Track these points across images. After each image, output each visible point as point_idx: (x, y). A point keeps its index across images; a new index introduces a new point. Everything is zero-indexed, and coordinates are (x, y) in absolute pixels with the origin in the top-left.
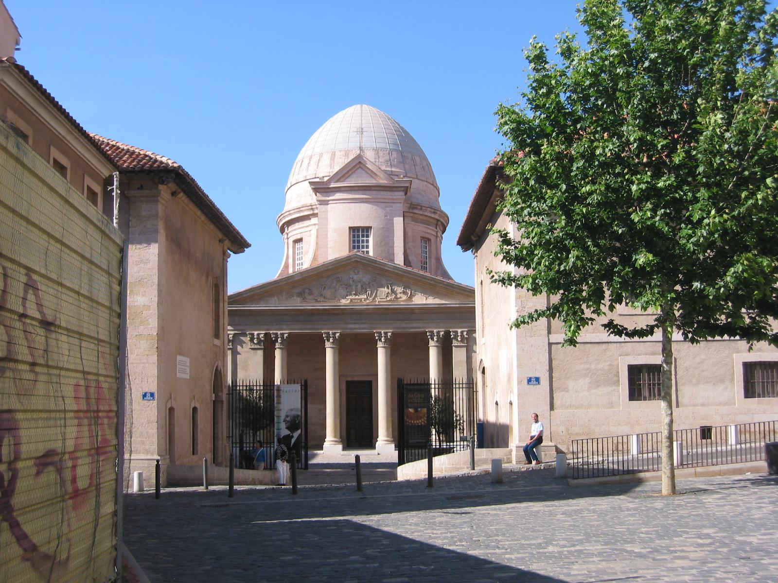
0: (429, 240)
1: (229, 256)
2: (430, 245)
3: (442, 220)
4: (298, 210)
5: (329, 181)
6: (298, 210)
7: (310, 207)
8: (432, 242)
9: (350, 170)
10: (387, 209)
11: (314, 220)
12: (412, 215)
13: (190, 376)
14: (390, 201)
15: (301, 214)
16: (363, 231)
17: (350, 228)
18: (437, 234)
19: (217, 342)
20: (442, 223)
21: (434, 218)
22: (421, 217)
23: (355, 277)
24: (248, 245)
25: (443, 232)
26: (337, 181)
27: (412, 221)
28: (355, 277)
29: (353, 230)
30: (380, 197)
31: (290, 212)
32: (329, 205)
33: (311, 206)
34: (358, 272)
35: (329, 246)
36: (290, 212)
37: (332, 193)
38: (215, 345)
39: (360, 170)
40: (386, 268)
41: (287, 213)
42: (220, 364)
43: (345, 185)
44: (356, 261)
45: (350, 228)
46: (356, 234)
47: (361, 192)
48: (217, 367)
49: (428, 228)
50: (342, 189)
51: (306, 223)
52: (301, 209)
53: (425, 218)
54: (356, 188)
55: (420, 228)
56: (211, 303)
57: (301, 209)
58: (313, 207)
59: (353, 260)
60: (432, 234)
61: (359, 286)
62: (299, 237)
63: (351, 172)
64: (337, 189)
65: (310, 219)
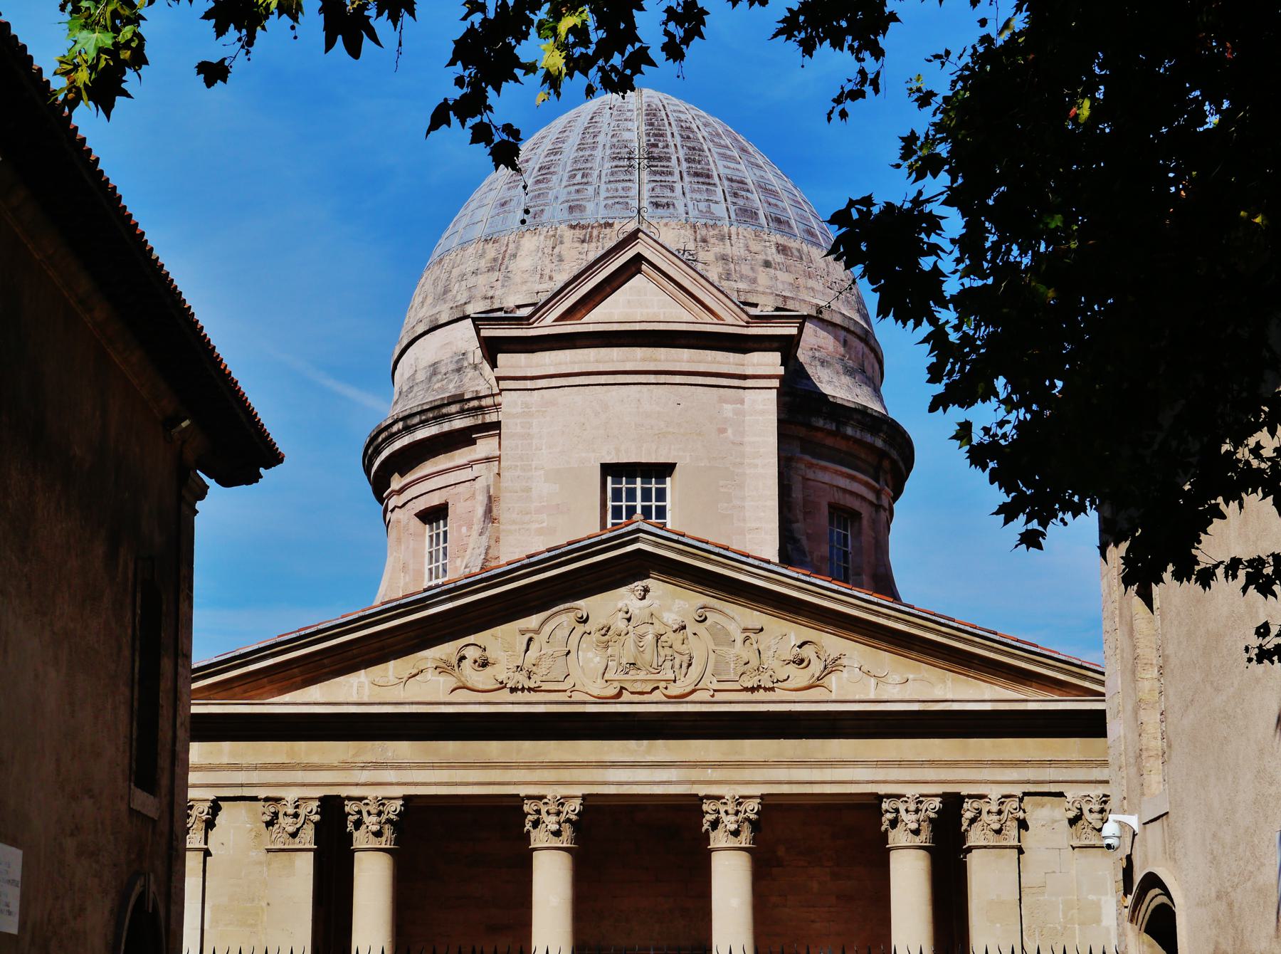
0: (855, 516)
1: (202, 492)
2: (858, 534)
3: (894, 454)
4: (436, 413)
6: (436, 413)
8: (865, 522)
11: (485, 446)
12: (802, 432)
13: (22, 925)
15: (446, 427)
18: (878, 498)
19: (145, 802)
20: (893, 462)
21: (871, 448)
22: (829, 441)
24: (274, 458)
25: (895, 498)
27: (804, 451)
34: (646, 590)
38: (139, 813)
41: (400, 425)
42: (153, 888)
44: (639, 550)
48: (142, 897)
49: (853, 478)
51: (461, 456)
52: (444, 411)
53: (842, 445)
55: (826, 477)
56: (127, 652)
57: (444, 411)
58: (484, 402)
60: (863, 498)
61: (650, 638)
65: (473, 442)
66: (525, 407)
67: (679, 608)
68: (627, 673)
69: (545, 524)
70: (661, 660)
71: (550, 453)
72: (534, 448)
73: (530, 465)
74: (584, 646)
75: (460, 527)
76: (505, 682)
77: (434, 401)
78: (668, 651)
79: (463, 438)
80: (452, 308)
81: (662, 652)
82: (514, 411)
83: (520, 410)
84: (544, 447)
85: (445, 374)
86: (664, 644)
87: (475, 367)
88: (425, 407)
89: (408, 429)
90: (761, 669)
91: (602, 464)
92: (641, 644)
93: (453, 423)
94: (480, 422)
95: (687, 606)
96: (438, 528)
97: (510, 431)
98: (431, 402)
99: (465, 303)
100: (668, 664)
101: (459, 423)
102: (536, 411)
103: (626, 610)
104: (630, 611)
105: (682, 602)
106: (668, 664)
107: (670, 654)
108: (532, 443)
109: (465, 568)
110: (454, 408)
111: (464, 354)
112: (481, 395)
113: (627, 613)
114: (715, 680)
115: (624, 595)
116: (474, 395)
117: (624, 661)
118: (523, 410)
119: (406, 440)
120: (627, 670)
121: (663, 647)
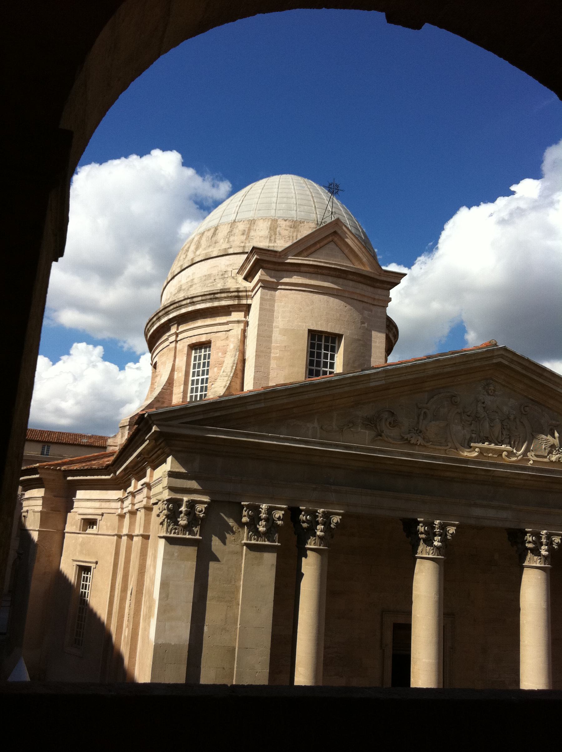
5: (287, 251)
7: (236, 294)
9: (319, 242)
10: (366, 312)
14: (370, 301)
15: (216, 304)
16: (327, 341)
17: (310, 331)
23: (488, 400)
26: (298, 255)
28: (488, 400)
29: (314, 335)
30: (358, 291)
31: (195, 300)
32: (278, 292)
33: (246, 291)
35: (272, 355)
36: (195, 300)
37: (288, 273)
39: (332, 245)
43: (311, 263)
45: (310, 331)
46: (316, 342)
47: (330, 278)
50: (303, 269)
54: (324, 271)
58: (241, 294)
59: (495, 361)
62: (203, 339)
63: (318, 246)
64: (295, 268)
66: (272, 297)
67: (512, 404)
69: (278, 355)
71: (283, 321)
73: (272, 325)
75: (218, 353)
76: (409, 439)
77: (213, 290)
79: (226, 311)
80: (219, 250)
81: (504, 433)
83: (268, 297)
84: (280, 317)
85: (215, 280)
87: (233, 278)
88: (206, 293)
89: (193, 303)
91: (308, 329)
93: (221, 302)
94: (236, 303)
96: (200, 352)
98: (210, 291)
99: (228, 248)
101: (224, 303)
103: (483, 401)
104: (486, 403)
109: (223, 372)
110: (223, 295)
111: (225, 272)
112: (240, 290)
116: (236, 290)
119: (190, 309)
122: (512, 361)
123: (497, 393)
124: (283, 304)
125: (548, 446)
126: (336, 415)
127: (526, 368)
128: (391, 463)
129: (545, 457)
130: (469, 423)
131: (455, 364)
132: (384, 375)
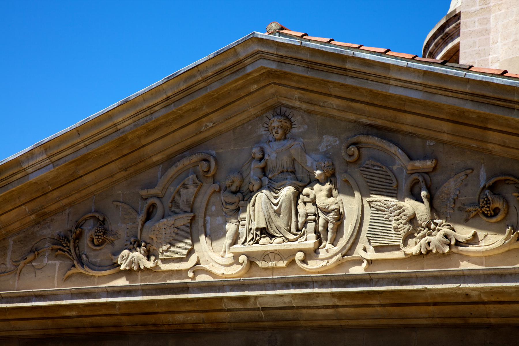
40: (393, 91)
66: (484, 4)
67: (327, 146)
68: (257, 243)
70: (301, 220)
71: (505, 44)
72: (491, 42)
73: (487, 60)
74: (213, 208)
78: (310, 208)
82: (473, 9)
83: (478, 7)
84: (499, 40)
86: (306, 199)
90: (433, 226)
92: (275, 201)
95: (338, 142)
97: (469, 29)
100: (311, 225)
102: (494, 6)
105: (331, 139)
106: (311, 225)
107: (313, 211)
108: (489, 38)
113: (261, 159)
114: (370, 249)
115: (262, 135)
117: (254, 226)
118: (481, 7)
120: (258, 238)
121: (305, 203)
122: (281, 60)
123: (295, 131)
124: (503, 11)
125: (404, 222)
126: (12, 243)
127: (311, 65)
128: (74, 313)
129: (397, 248)
130: (233, 207)
131: (168, 98)
132: (45, 156)
